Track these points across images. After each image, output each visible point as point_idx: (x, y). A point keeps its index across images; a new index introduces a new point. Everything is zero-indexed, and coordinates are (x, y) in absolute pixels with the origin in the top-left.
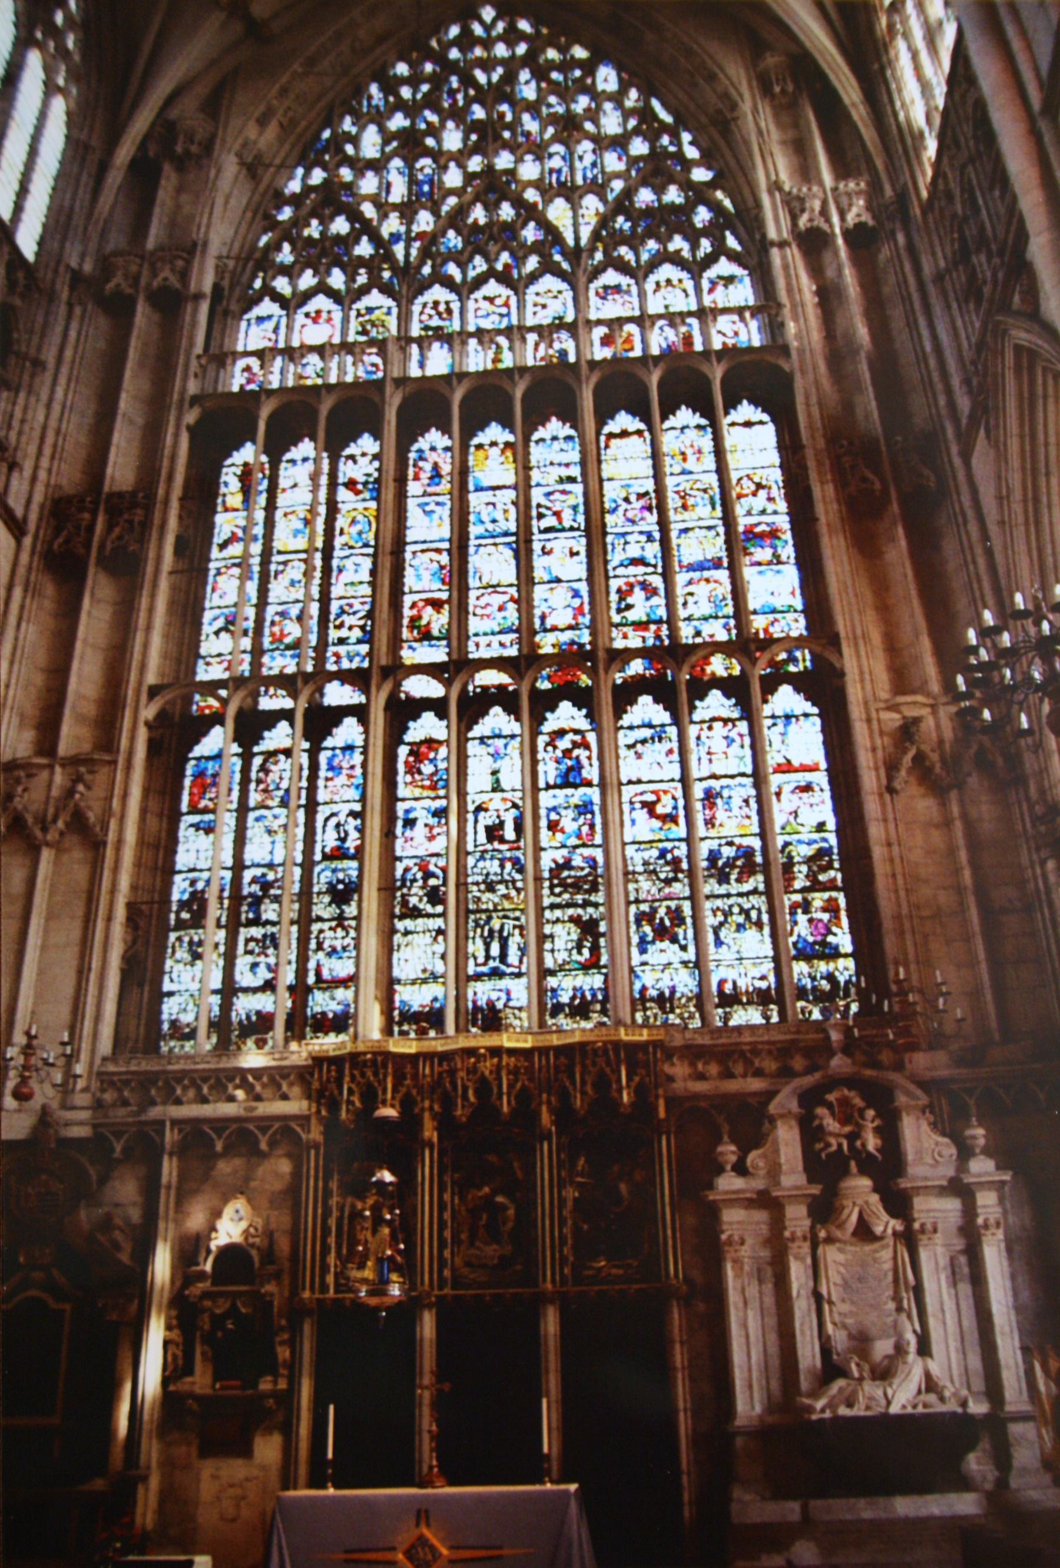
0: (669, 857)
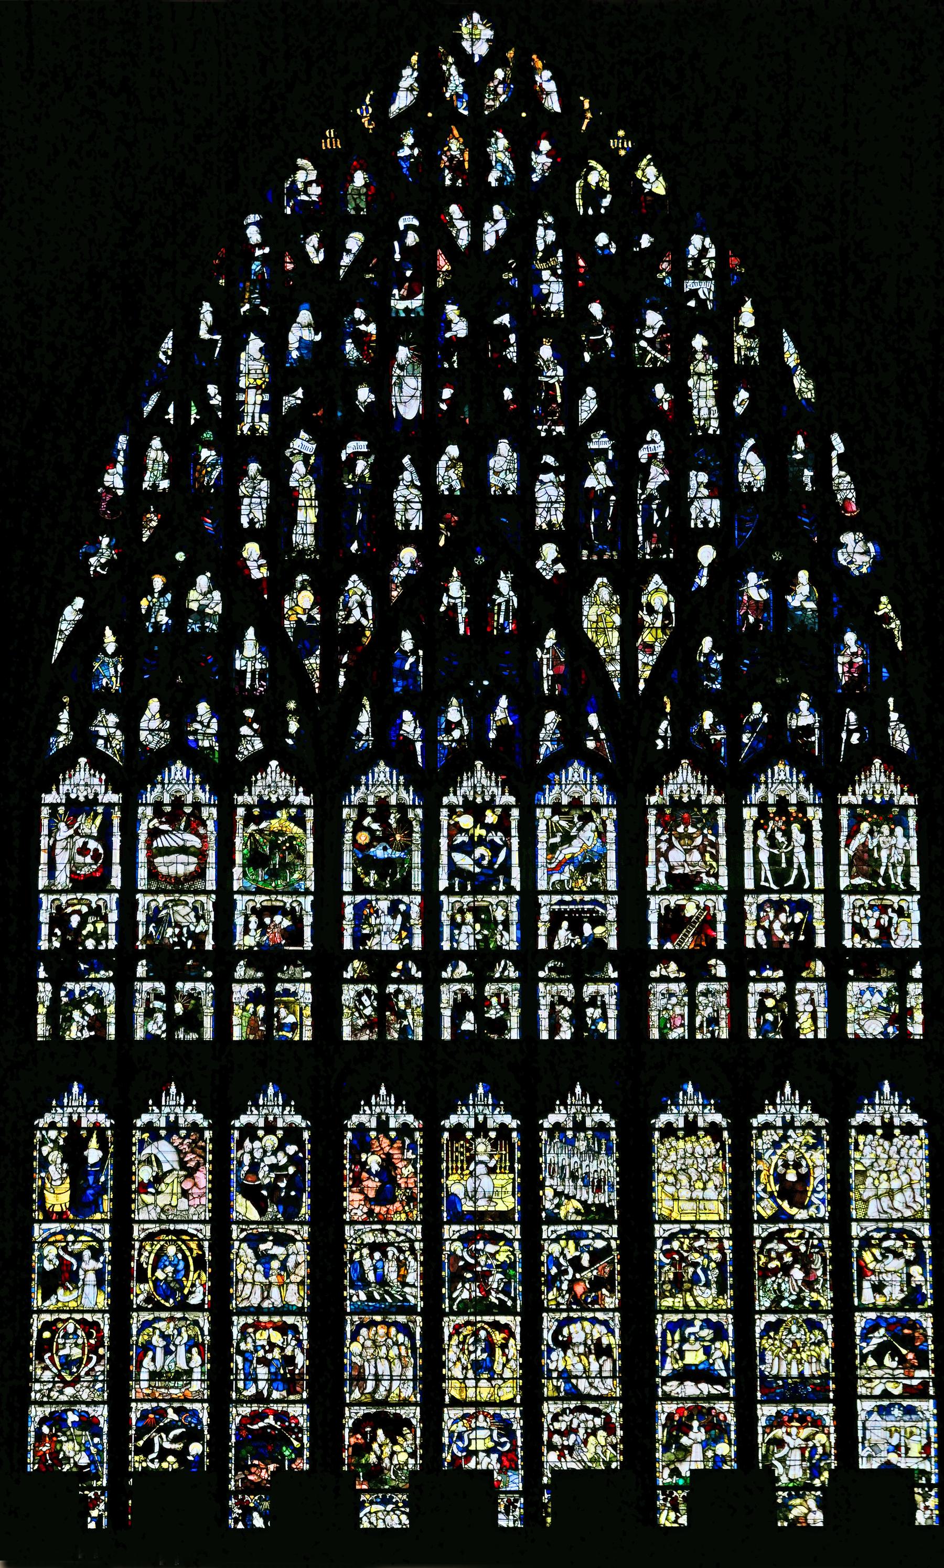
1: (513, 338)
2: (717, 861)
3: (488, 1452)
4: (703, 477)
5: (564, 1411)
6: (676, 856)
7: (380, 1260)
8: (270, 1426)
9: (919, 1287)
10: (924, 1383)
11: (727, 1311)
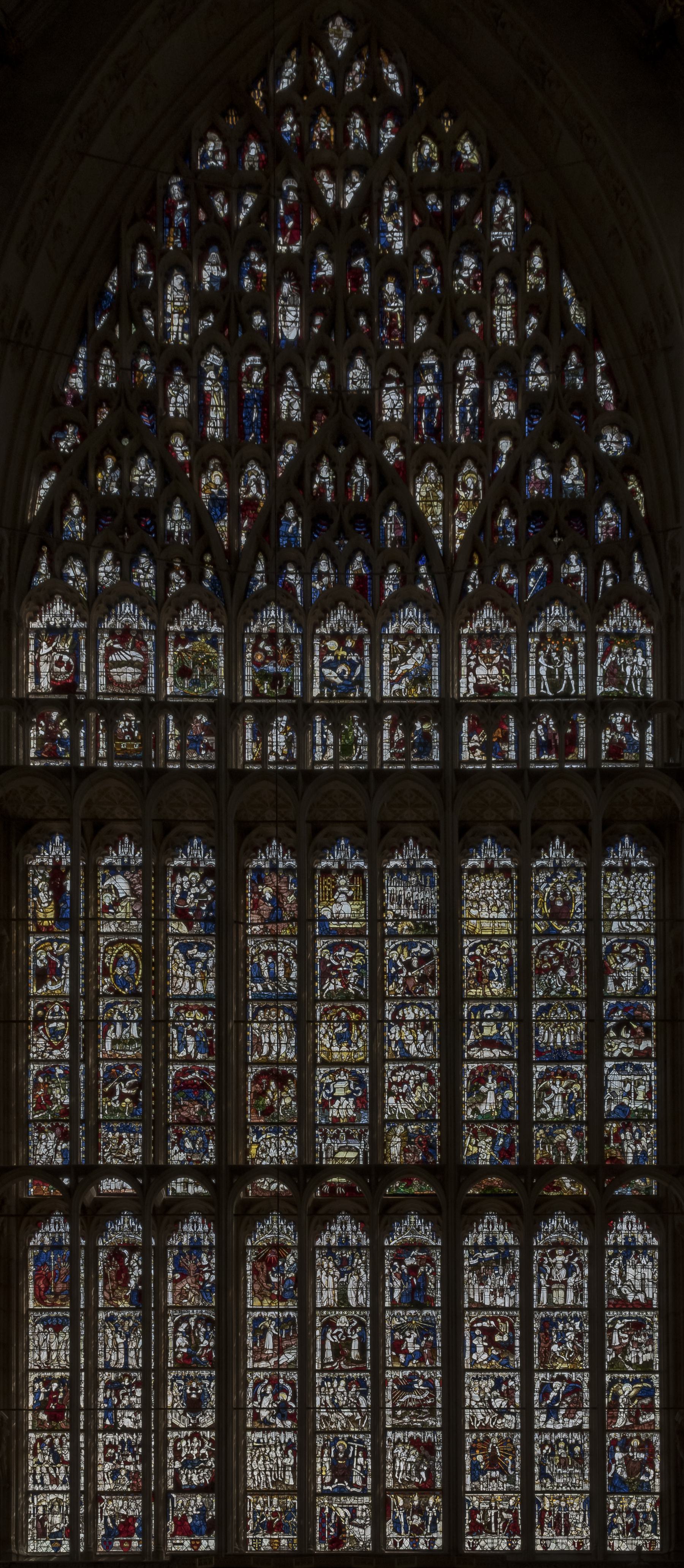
0: (504, 1388)
1: (366, 278)
2: (510, 674)
3: (347, 1097)
4: (503, 385)
5: (399, 1069)
6: (481, 671)
8: (196, 1078)
9: (647, 981)
10: (648, 1049)
11: (513, 999)
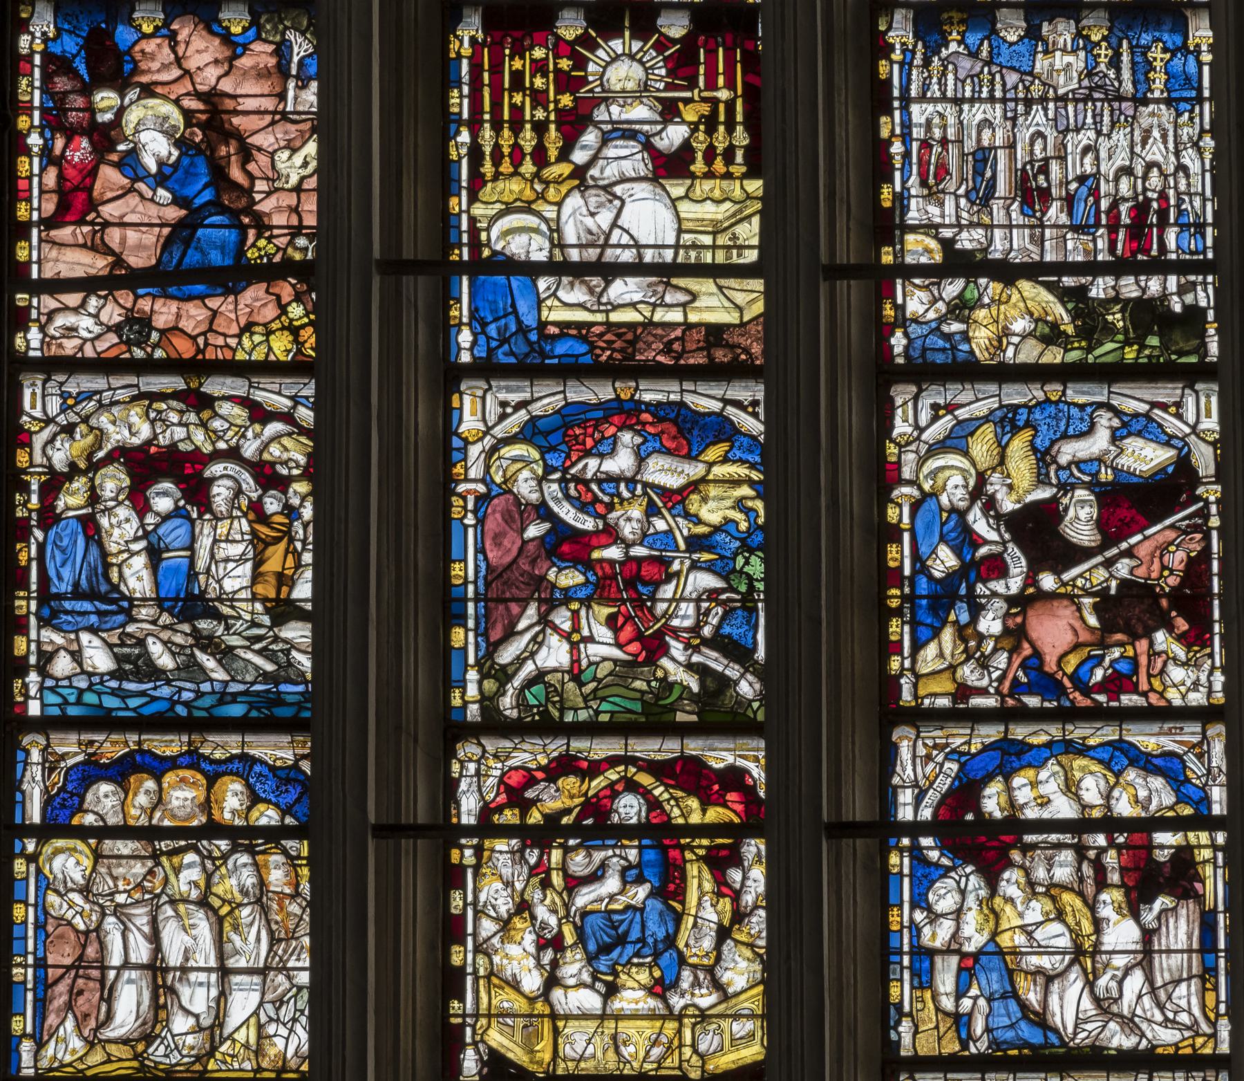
7: (177, 513)
